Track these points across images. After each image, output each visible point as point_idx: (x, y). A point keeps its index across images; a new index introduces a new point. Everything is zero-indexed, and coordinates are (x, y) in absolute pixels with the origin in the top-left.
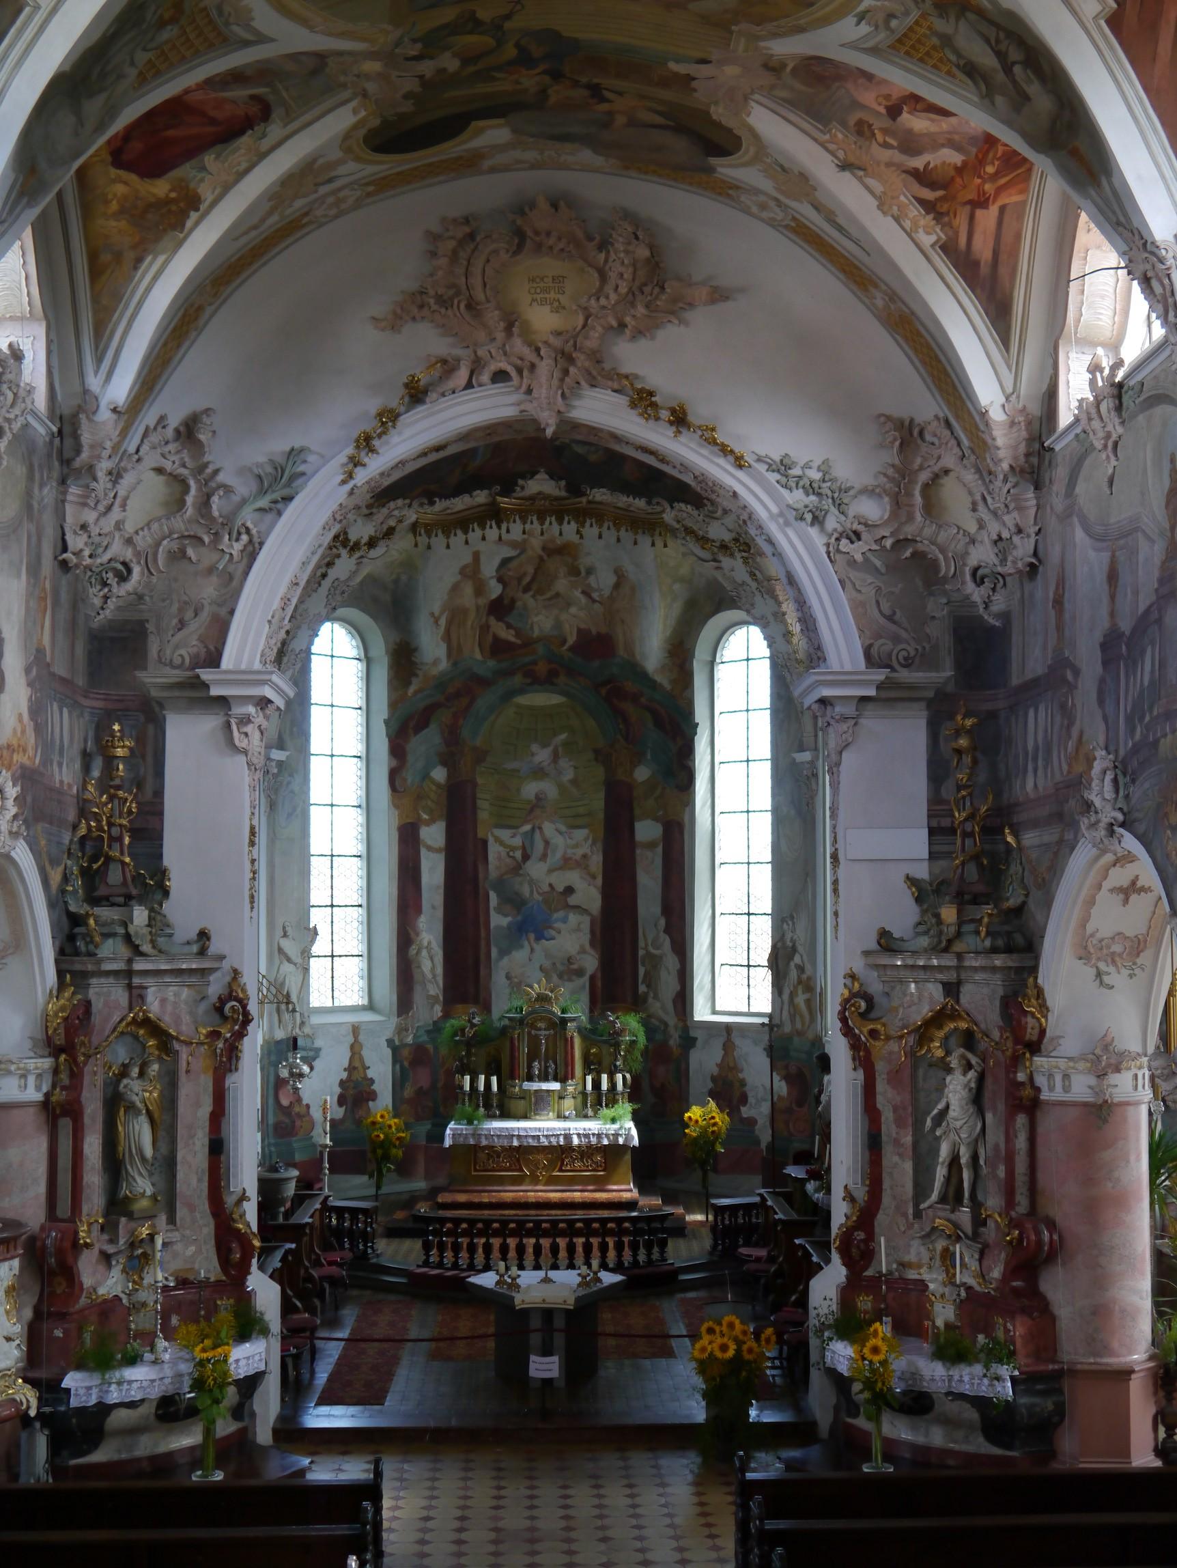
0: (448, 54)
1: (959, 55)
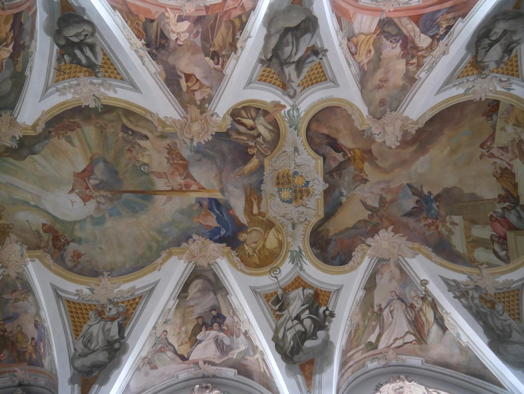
1: (503, 57)
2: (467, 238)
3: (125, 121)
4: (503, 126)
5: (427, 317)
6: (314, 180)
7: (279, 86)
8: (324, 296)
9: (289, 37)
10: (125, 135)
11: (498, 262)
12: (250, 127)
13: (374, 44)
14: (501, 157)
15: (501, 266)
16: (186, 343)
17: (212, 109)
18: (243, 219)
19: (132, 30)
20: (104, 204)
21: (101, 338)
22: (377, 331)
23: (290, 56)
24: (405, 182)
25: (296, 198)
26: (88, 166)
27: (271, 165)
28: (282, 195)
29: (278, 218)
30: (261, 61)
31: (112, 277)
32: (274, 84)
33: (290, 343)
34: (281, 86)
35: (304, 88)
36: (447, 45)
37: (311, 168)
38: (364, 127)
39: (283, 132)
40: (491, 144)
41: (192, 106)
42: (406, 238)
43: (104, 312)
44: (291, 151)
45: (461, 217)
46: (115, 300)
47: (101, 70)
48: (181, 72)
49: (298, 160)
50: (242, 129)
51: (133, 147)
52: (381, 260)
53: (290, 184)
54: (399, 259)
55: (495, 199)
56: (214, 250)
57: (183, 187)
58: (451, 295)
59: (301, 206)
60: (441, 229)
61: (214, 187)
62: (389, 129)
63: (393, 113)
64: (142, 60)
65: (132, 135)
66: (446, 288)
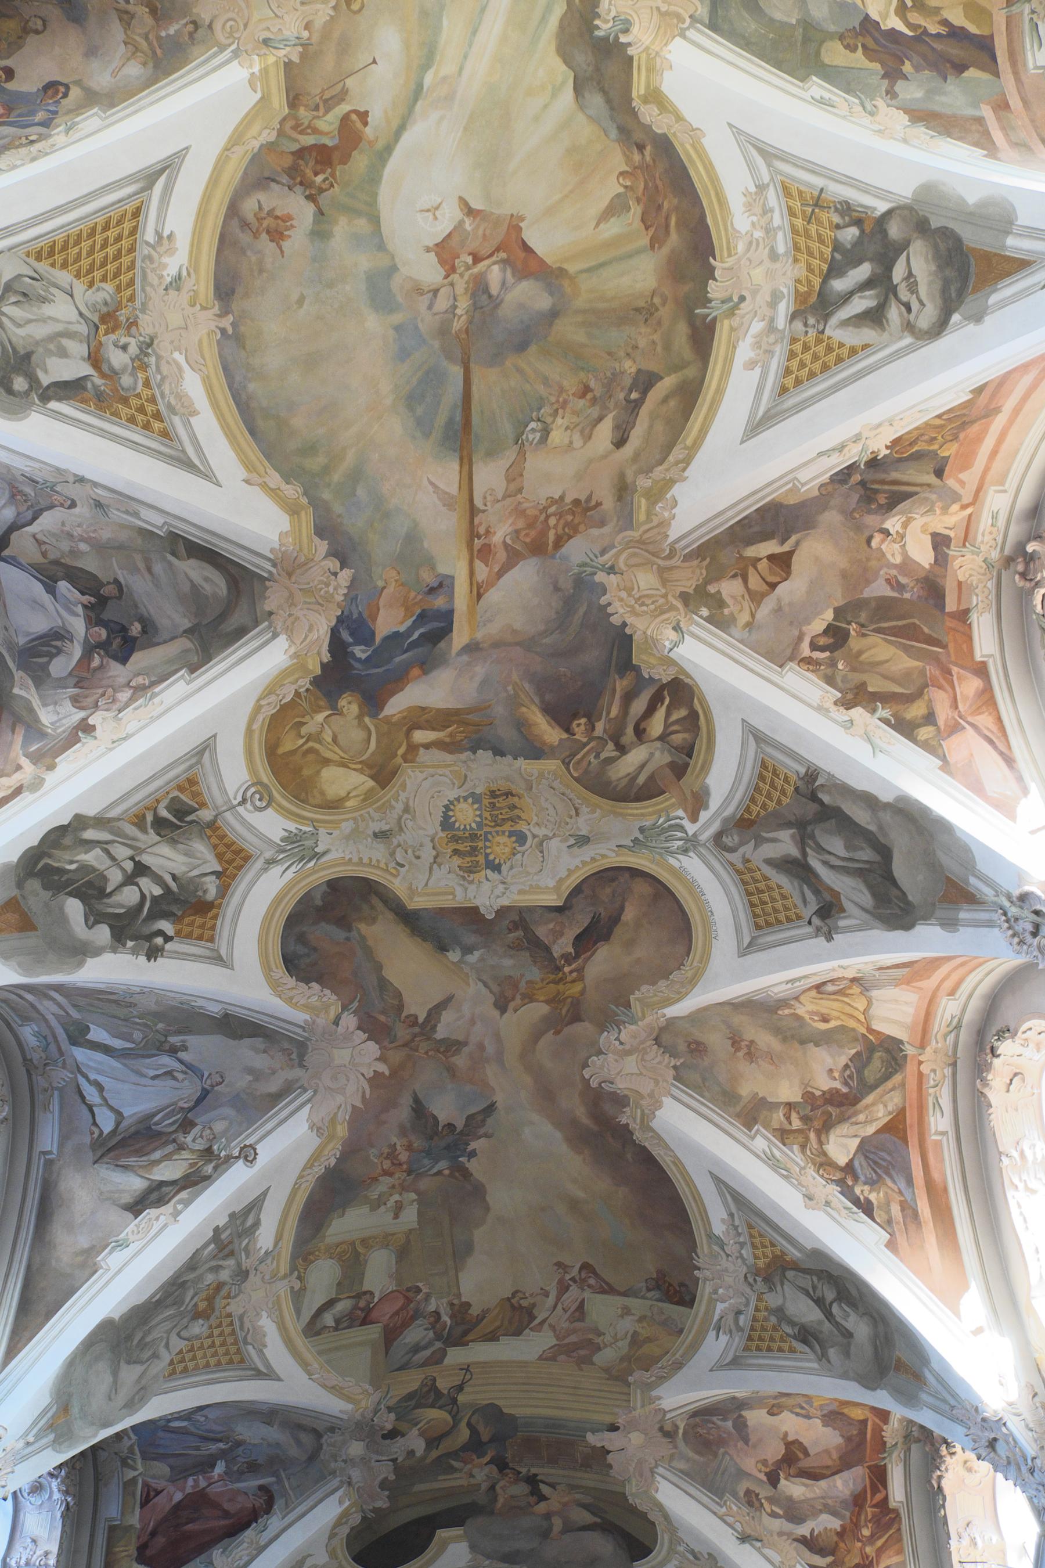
0: (415, 1432)
1: (792, 1323)
2: (364, 1241)
4: (633, 1311)
5: (163, 1164)
6: (504, 883)
7: (748, 810)
8: (202, 926)
9: (866, 854)
10: (628, 381)
11: (307, 1315)
12: (641, 727)
13: (842, 1029)
14: (559, 1306)
15: (298, 1319)
16: (44, 554)
17: (694, 629)
18: (397, 705)
19: (917, 428)
20: (430, 307)
21: (39, 331)
22: (117, 1043)
23: (820, 849)
24: (499, 1098)
25: (455, 839)
26: (542, 262)
27: (541, 775)
28: (463, 805)
29: (403, 796)
30: (812, 775)
31: (218, 342)
32: (753, 800)
33: (72, 862)
34: (746, 816)
35: (737, 871)
36: (828, 1203)
37: (535, 878)
38: (636, 1007)
39: (630, 811)
40: (589, 1286)
41: (704, 572)
42: (359, 1104)
43: (113, 331)
44: (579, 829)
45: (415, 1225)
46: (153, 360)
47: (812, 333)
48: (798, 543)
49: (554, 845)
50: (639, 706)
51: (594, 401)
52: (302, 1047)
53: (493, 824)
54: (305, 1090)
55: (459, 1295)
56: (311, 629)
57: (482, 541)
58: (222, 1221)
59: (434, 853)
60: (384, 1184)
61: (485, 625)
62: (631, 1063)
63: (672, 1072)
65: (627, 400)
66: (238, 1208)
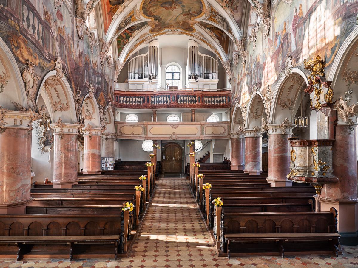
3: (147, 3)
64: (126, 7)
